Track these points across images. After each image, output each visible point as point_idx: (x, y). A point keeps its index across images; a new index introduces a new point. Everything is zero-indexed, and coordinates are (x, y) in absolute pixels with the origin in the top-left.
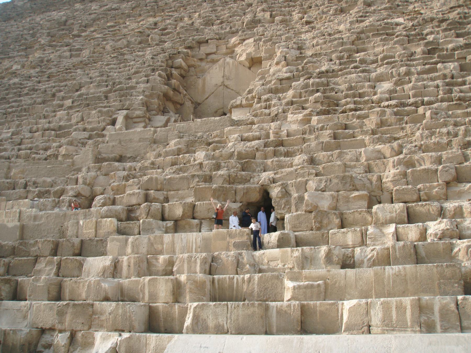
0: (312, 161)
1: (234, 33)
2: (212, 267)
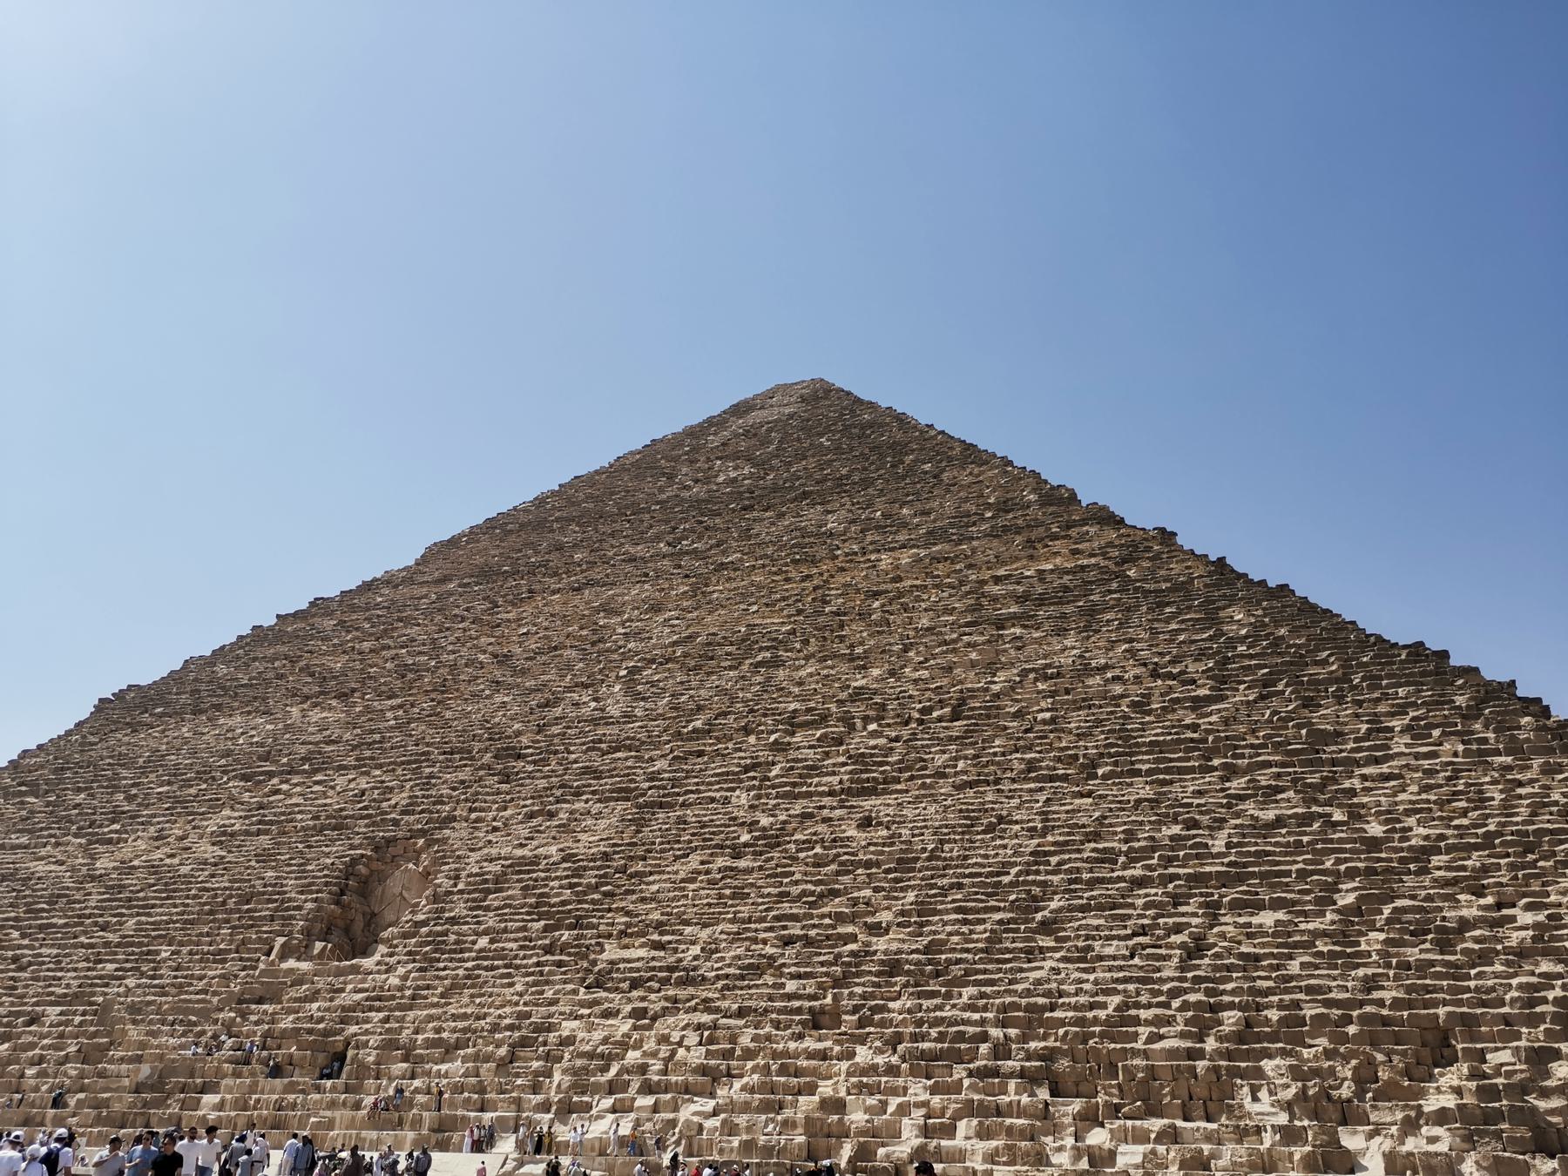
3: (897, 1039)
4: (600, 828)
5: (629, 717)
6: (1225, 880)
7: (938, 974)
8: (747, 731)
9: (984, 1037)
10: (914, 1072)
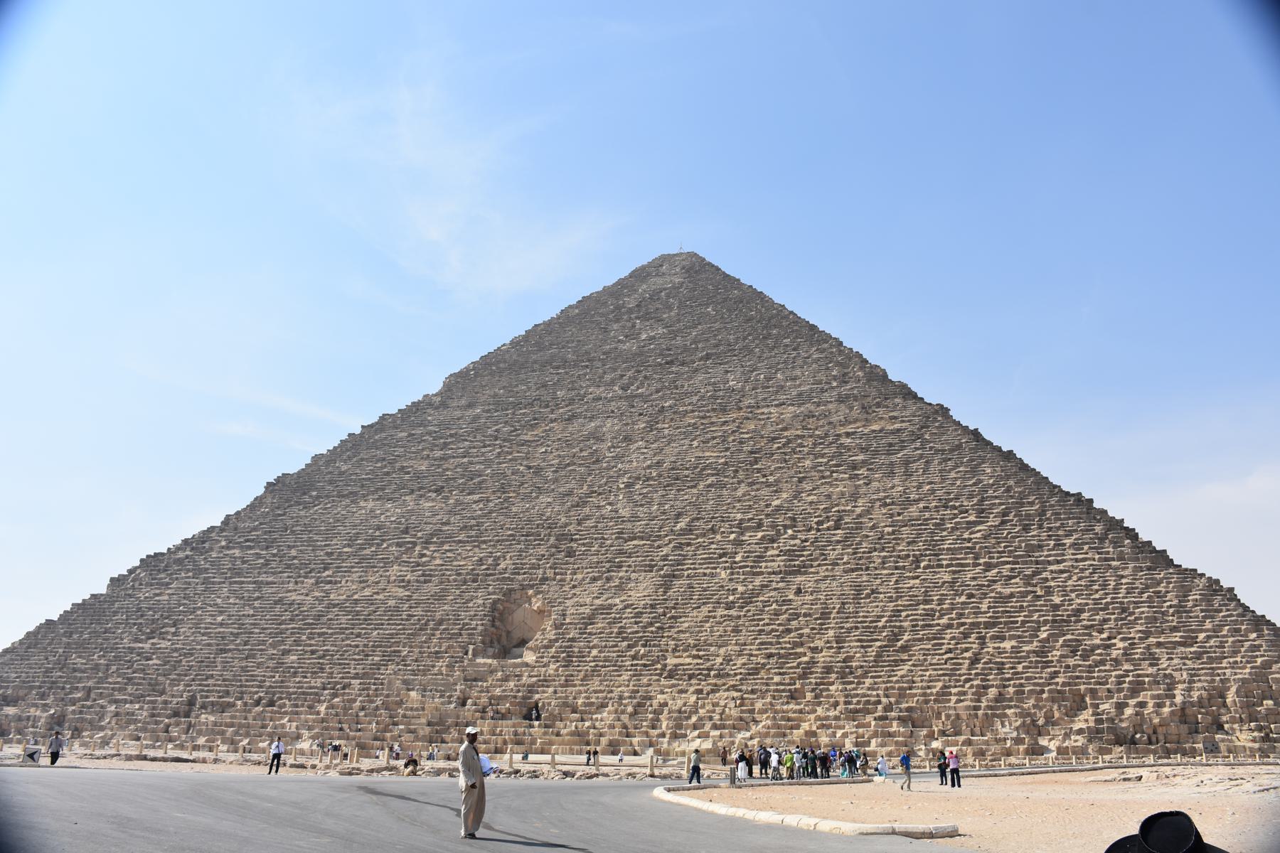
0: (555, 692)
1: (532, 587)
2: (516, 734)
3: (836, 704)
4: (642, 589)
5: (635, 518)
6: (988, 625)
7: (851, 673)
8: (713, 530)
9: (879, 702)
10: (847, 719)
